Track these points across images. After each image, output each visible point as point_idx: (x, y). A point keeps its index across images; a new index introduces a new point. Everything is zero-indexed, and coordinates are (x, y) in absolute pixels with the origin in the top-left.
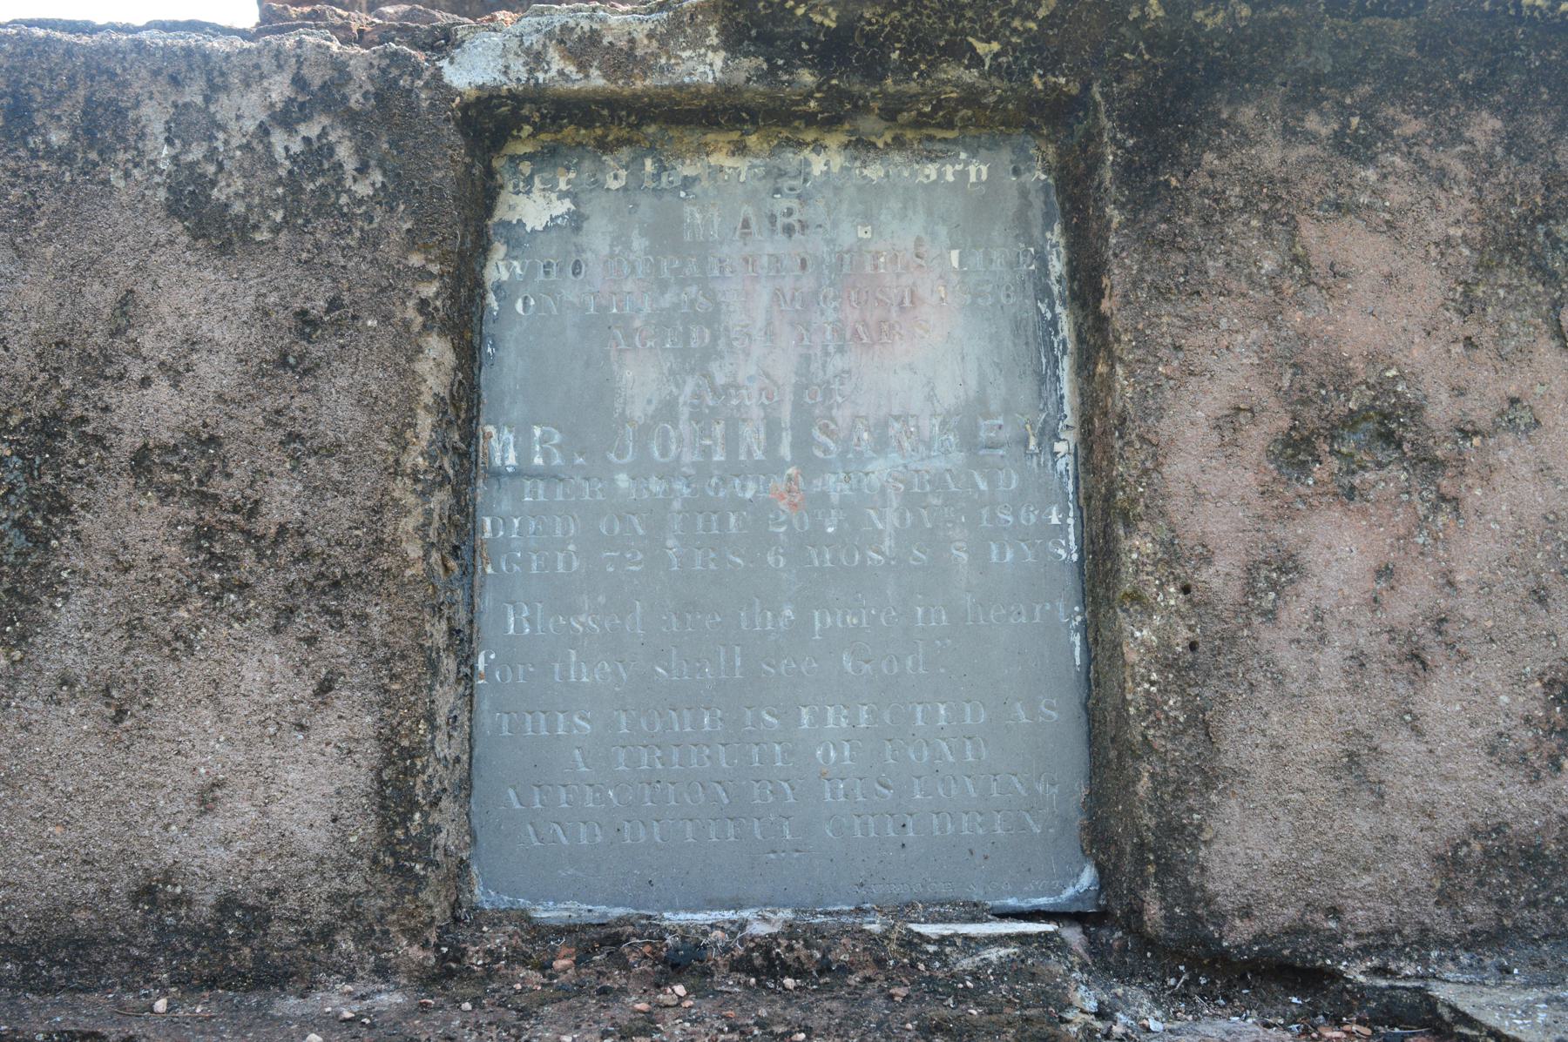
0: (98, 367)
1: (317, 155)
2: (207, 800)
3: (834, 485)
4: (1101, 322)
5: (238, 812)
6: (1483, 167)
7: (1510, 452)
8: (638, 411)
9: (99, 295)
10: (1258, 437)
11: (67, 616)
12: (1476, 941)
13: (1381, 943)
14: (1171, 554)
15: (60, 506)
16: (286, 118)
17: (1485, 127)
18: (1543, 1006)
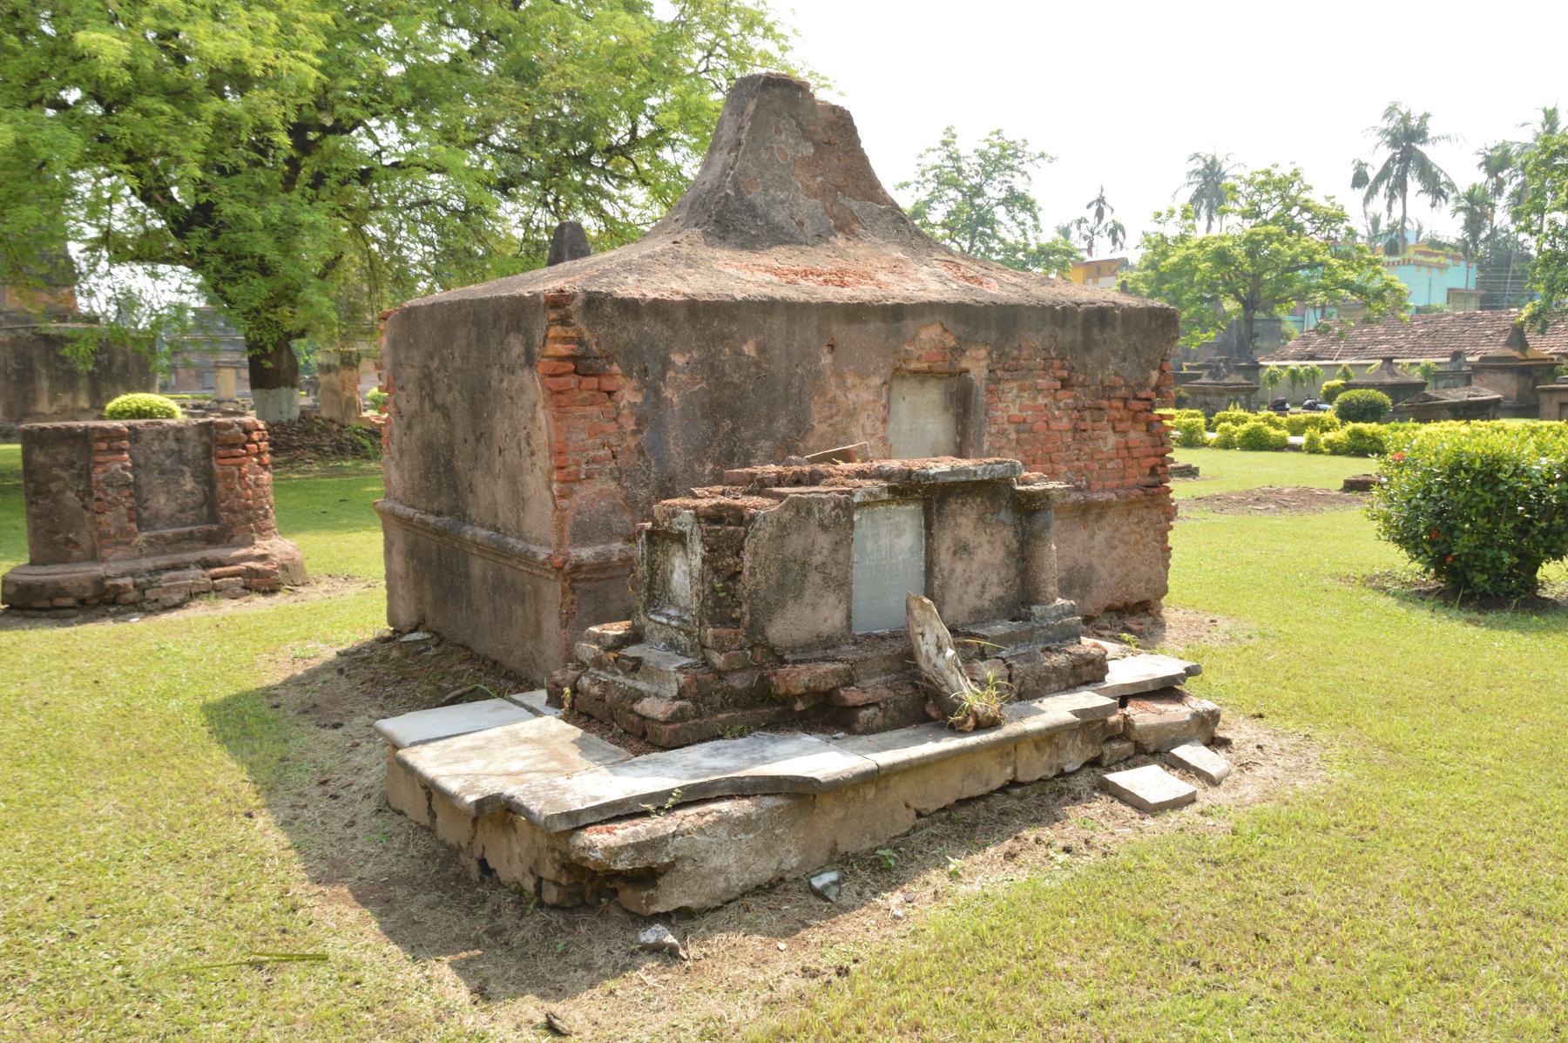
0: (810, 553)
1: (838, 516)
2: (825, 621)
3: (894, 561)
4: (932, 535)
5: (830, 621)
6: (978, 506)
7: (979, 551)
8: (869, 550)
9: (810, 541)
10: (951, 551)
11: (807, 593)
12: (974, 623)
13: (962, 625)
14: (941, 570)
15: (805, 576)
16: (833, 509)
17: (979, 500)
18: (1001, 628)
